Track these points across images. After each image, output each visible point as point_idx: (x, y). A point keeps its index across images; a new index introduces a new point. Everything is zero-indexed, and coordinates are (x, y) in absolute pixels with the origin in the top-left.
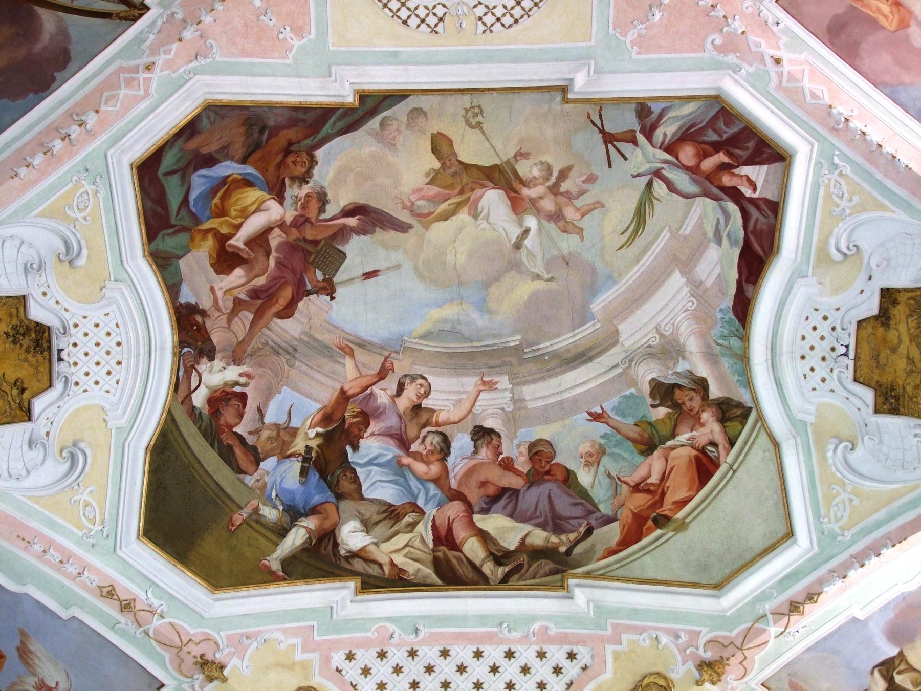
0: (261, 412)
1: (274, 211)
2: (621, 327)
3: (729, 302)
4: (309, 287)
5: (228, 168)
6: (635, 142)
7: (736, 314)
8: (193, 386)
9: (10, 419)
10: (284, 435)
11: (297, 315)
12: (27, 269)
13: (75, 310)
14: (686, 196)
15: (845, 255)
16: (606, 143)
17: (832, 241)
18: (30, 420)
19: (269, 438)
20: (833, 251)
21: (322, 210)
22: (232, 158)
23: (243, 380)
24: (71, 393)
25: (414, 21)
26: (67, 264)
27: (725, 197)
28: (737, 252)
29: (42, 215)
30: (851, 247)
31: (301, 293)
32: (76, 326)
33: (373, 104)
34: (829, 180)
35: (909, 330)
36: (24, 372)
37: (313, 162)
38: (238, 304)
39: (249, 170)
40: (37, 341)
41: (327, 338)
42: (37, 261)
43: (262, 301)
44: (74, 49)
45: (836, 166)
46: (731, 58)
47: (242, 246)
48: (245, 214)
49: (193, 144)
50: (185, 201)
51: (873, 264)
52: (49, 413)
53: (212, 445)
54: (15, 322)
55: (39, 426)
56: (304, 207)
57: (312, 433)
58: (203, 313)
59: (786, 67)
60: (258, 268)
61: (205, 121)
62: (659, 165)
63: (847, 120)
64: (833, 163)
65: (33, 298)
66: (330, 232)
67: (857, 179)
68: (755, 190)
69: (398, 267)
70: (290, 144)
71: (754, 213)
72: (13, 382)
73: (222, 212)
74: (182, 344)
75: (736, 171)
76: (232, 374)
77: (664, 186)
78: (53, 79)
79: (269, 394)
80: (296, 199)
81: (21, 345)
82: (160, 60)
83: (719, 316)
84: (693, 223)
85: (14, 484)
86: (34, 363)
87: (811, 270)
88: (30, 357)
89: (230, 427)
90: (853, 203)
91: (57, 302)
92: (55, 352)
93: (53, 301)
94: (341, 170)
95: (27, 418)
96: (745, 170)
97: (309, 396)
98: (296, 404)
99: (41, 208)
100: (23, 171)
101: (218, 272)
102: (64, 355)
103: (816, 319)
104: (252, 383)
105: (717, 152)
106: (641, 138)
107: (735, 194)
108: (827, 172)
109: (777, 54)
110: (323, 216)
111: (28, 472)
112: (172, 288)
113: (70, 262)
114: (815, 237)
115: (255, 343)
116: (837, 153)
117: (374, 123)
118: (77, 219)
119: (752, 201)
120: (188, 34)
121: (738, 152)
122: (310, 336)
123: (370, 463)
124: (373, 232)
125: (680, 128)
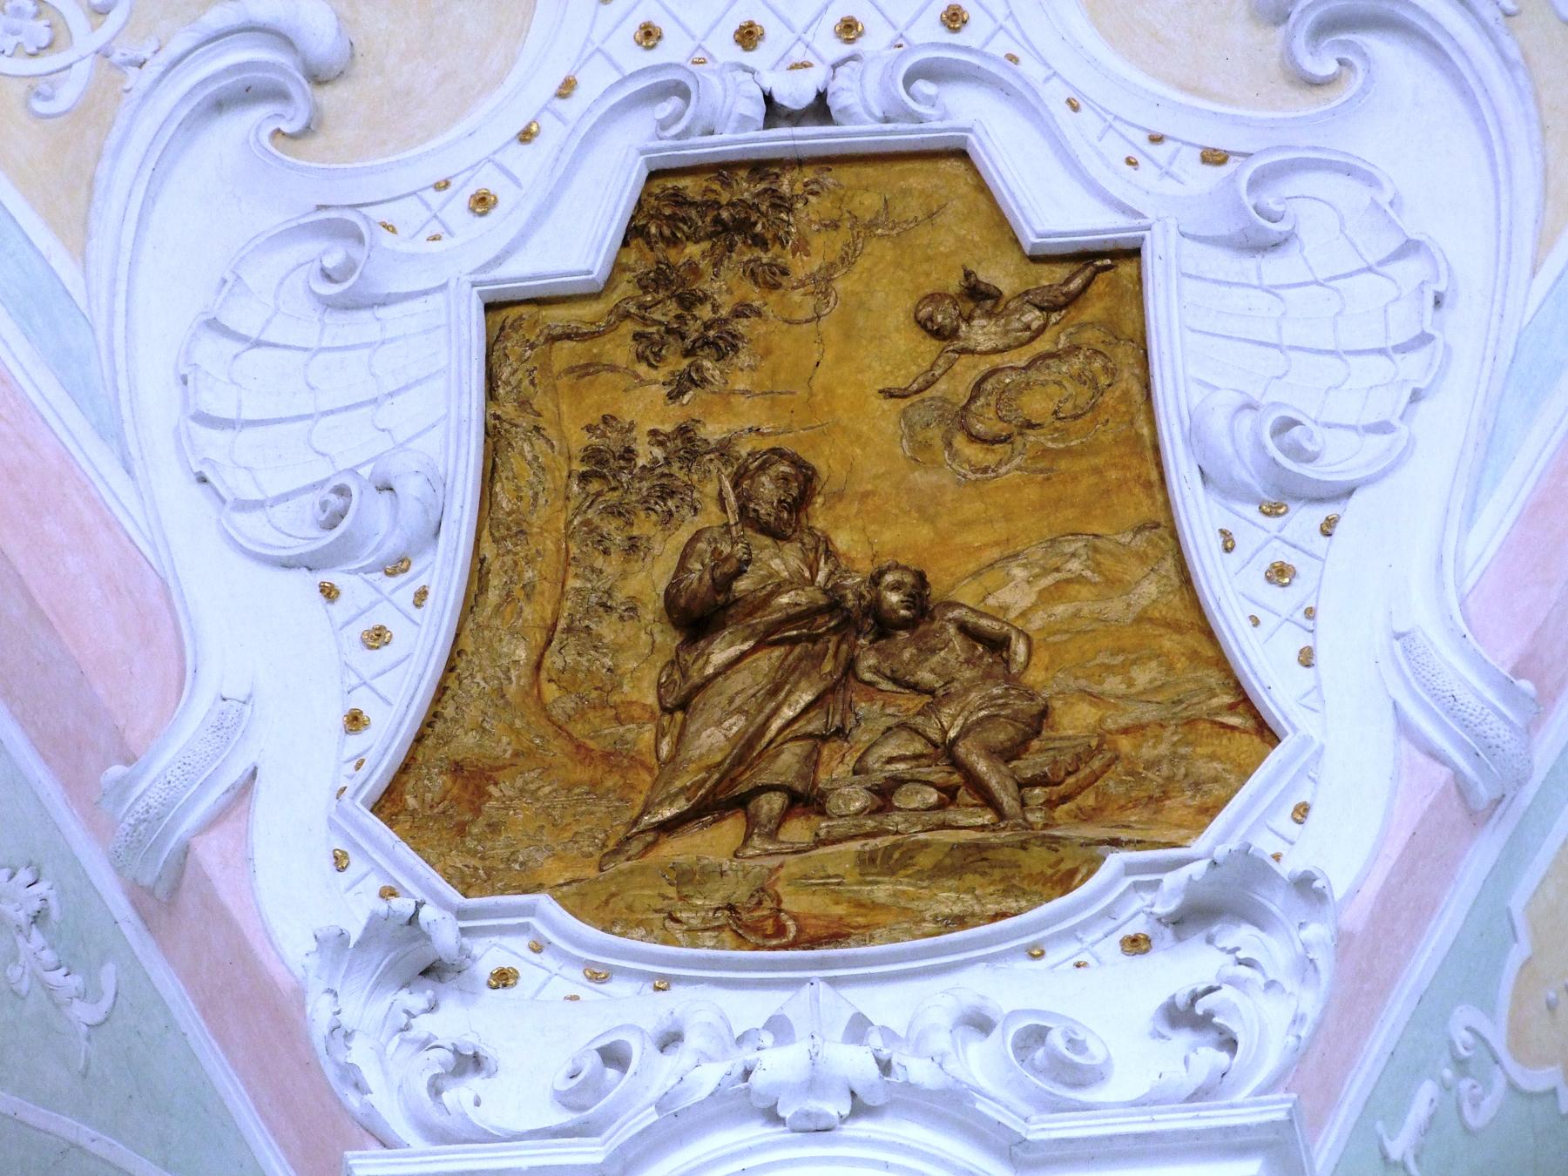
9: (1124, 355)
12: (349, 296)
13: (573, 39)
18: (1133, 253)
24: (1001, 46)
26: (329, 97)
29: (77, 232)
32: (649, 35)
36: (884, 294)
40: (712, 226)
42: (311, 248)
52: (1103, 154)
54: (619, 349)
55: (1166, 209)
65: (498, 260)
72: (931, 346)
81: (743, 310)
85: (1464, 329)
86: (839, 240)
88: (802, 267)
91: (526, 136)
92: (784, 138)
93: (526, 161)
95: (1126, 269)
99: (44, 239)
102: (795, 91)
111: (1410, 248)
113: (317, 78)
118: (103, 53)
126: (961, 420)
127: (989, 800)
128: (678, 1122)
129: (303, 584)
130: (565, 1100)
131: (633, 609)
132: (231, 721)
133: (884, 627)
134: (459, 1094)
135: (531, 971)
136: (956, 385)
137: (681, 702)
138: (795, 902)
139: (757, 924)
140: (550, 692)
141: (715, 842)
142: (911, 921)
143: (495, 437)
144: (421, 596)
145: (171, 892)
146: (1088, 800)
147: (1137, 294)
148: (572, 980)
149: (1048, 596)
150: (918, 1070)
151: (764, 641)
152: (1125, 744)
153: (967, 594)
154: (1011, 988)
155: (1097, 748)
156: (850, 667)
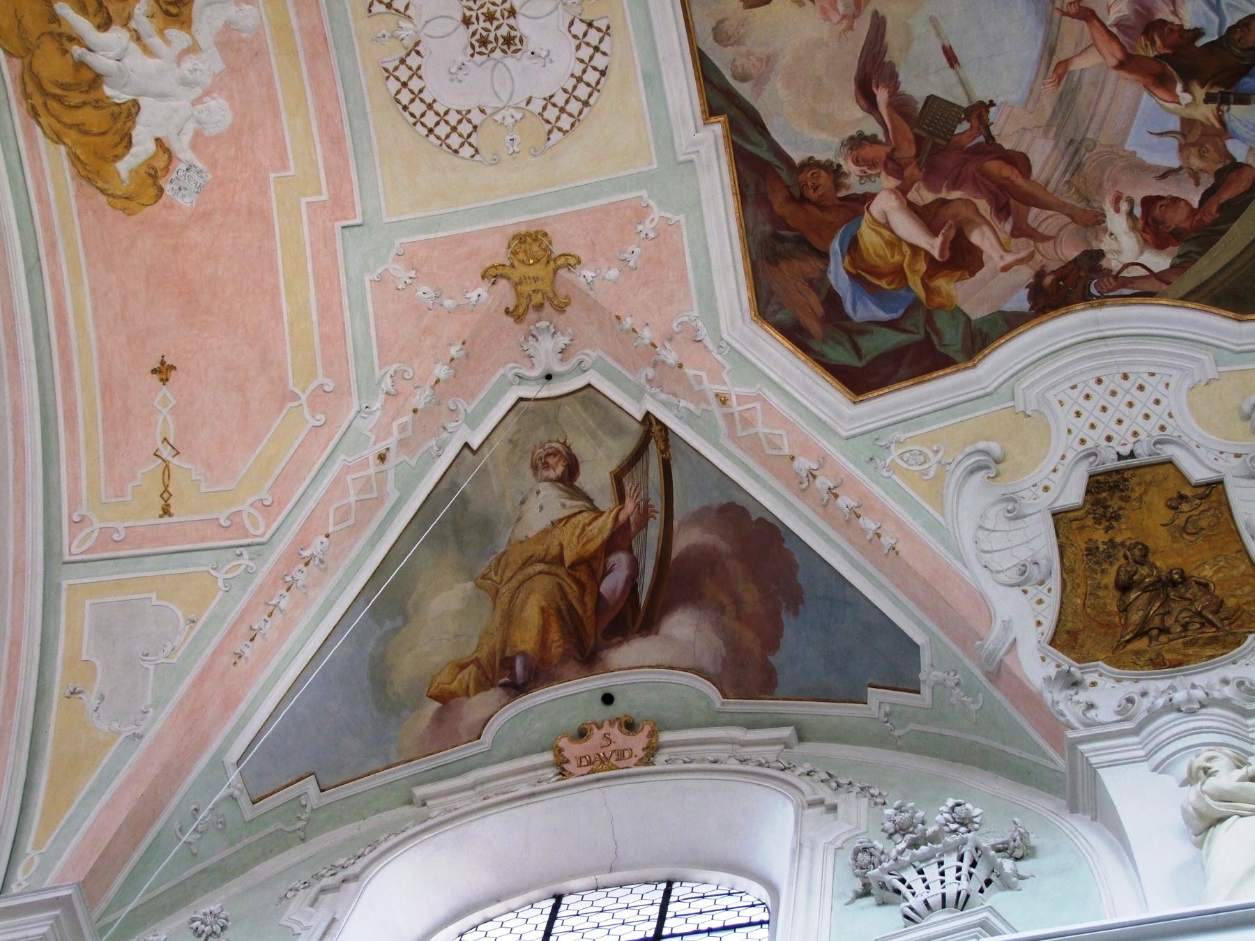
0: (1166, 174)
1: (886, 204)
4: (981, 139)
5: (838, 275)
8: (1143, 272)
9: (1224, 509)
10: (1191, 135)
11: (1023, 149)
12: (1016, 516)
13: (1062, 445)
18: (1221, 482)
19: (1202, 156)
21: (873, 140)
22: (824, 272)
23: (1124, 207)
24: (1176, 434)
25: (599, 61)
26: (1001, 467)
29: (940, 507)
31: (991, 148)
32: (1083, 441)
33: (720, 97)
37: (810, 164)
38: (1021, 230)
39: (835, 246)
40: (1110, 488)
41: (1048, 103)
42: (1003, 505)
43: (1012, 200)
44: (718, 499)
47: (939, 240)
48: (896, 242)
49: (814, 327)
50: (891, 325)
52: (1209, 458)
53: (1223, 233)
54: (1089, 521)
55: (1228, 469)
56: (872, 164)
57: (1186, 98)
58: (1040, 275)
60: (965, 212)
61: (780, 317)
66: (900, 122)
69: (933, 21)
70: (791, 198)
72: (1171, 513)
73: (898, 274)
74: (1086, 298)
76: (1117, 222)
78: (761, 521)
79: (1139, 168)
80: (864, 177)
81: (1120, 508)
82: (711, 388)
89: (1193, 212)
91: (1055, 471)
92: (1123, 463)
93: (1055, 477)
94: (814, 124)
95: (1220, 487)
97: (1134, 112)
98: (1146, 127)
99: (931, 511)
100: (887, 541)
101: (981, 265)
102: (1125, 451)
104: (1127, 193)
110: (881, 137)
112: (1011, 323)
113: (997, 462)
115: (1070, 199)
117: (744, 90)
118: (939, 462)
120: (671, 357)
122: (1049, 125)
123: (1216, 9)
124: (892, 65)
126: (1184, 529)
127: (1214, 625)
128: (1153, 715)
129: (1018, 590)
130: (1118, 713)
131: (1106, 587)
132: (1007, 626)
133: (1174, 584)
134: (1091, 714)
135: (1101, 682)
136: (1181, 520)
137: (1125, 609)
138: (1168, 656)
139: (1158, 663)
140: (1089, 610)
141: (1142, 643)
142: (1200, 658)
143: (1061, 548)
144: (1050, 590)
145: (999, 672)
146: (1239, 622)
147: (1224, 492)
148: (1111, 683)
149: (1216, 572)
150: (1216, 695)
151: (1144, 591)
152: (1246, 607)
153: (1195, 573)
154: (1232, 672)
155: (1238, 609)
156: (1168, 596)
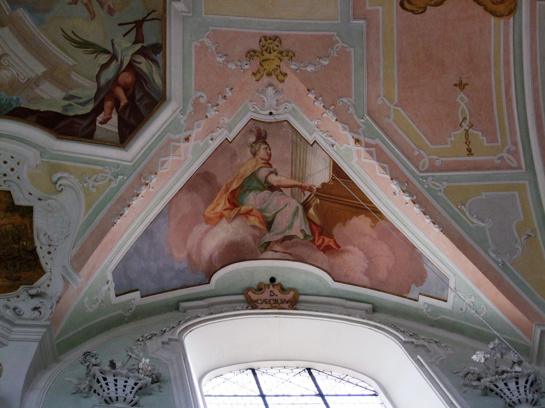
2: (6, 30)
3: (24, 104)
6: (135, 43)
7: (16, 109)
14: (98, 77)
15: (56, 183)
16: (135, 22)
17: (66, 175)
20: (59, 175)
27: (97, 103)
28: (59, 110)
30: (61, 187)
34: (107, 173)
35: (4, 225)
45: (116, 177)
46: (190, 108)
51: (49, 201)
59: (183, 145)
62: (119, 58)
63: (147, 184)
64: (118, 175)
67: (108, 190)
68: (102, 123)
71: (85, 123)
75: (114, 111)
77: (104, 62)
83: (14, 98)
84: (79, 81)
87: (46, 160)
90: (91, 189)
96: (115, 117)
103: (12, 164)
105: (128, 98)
106: (138, 46)
107: (98, 110)
108: (112, 171)
109: (192, 139)
114: (68, 163)
116: (125, 178)
119: (94, 120)
121: (128, 111)
125: (144, 73)
